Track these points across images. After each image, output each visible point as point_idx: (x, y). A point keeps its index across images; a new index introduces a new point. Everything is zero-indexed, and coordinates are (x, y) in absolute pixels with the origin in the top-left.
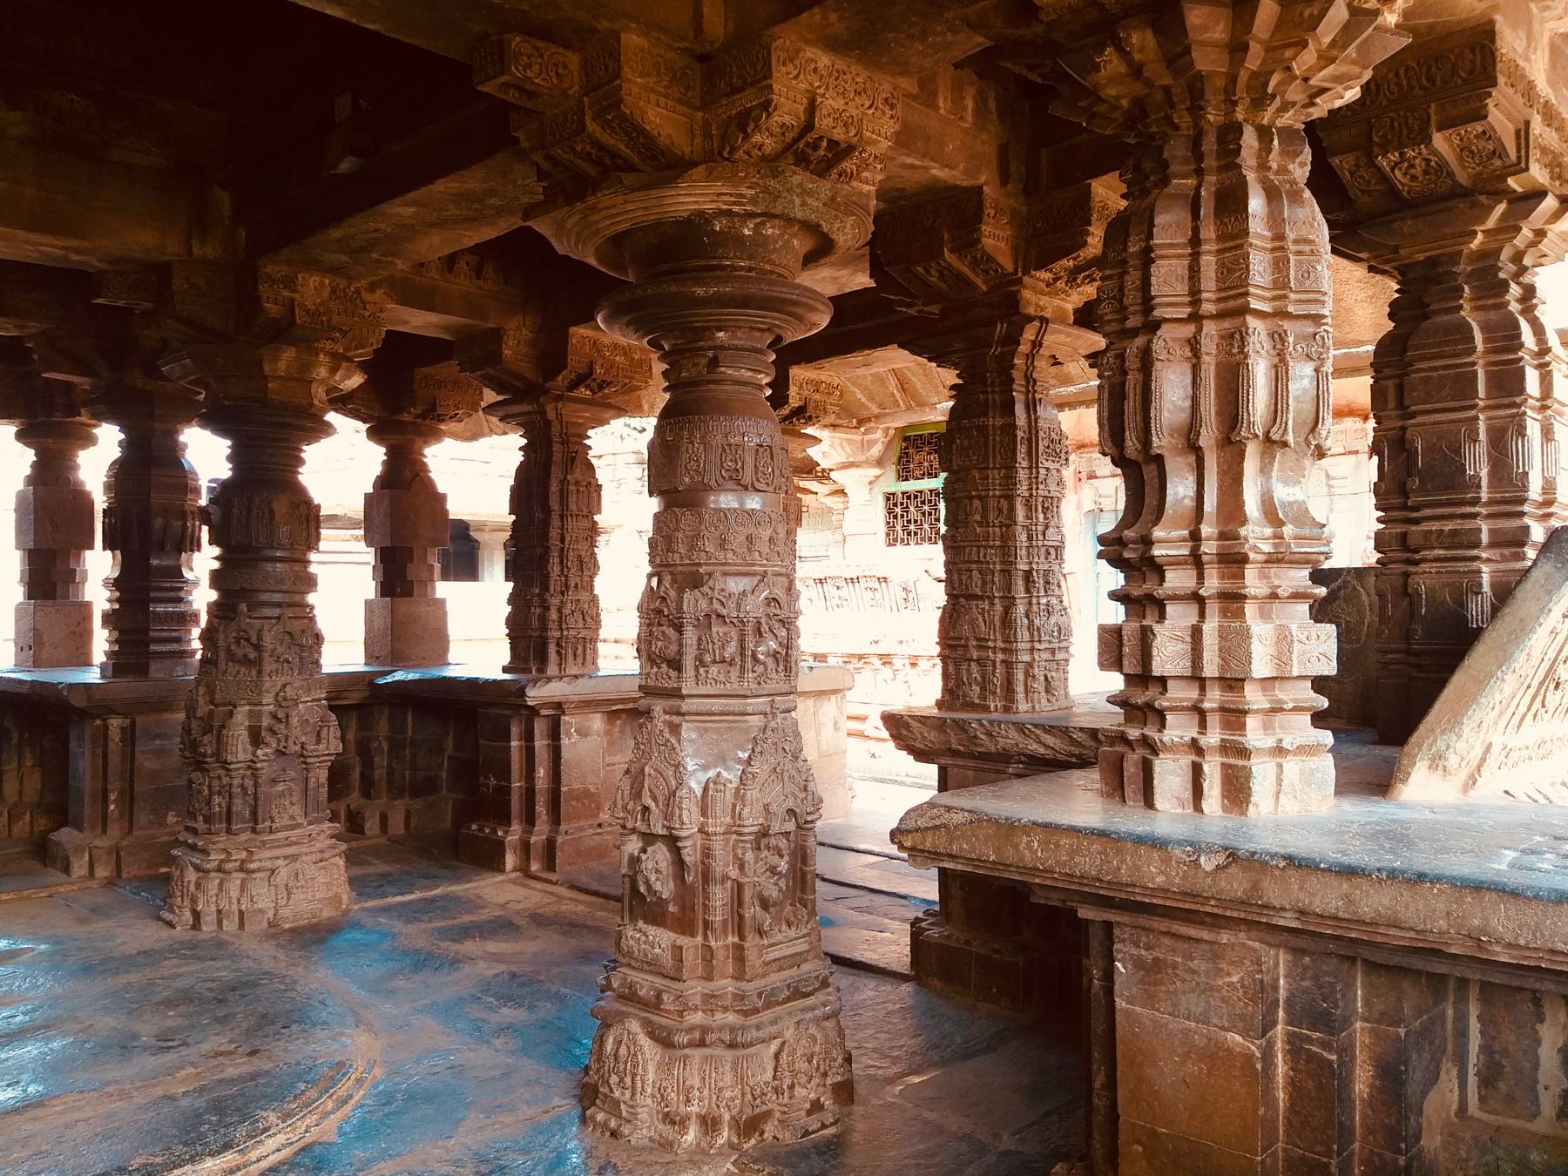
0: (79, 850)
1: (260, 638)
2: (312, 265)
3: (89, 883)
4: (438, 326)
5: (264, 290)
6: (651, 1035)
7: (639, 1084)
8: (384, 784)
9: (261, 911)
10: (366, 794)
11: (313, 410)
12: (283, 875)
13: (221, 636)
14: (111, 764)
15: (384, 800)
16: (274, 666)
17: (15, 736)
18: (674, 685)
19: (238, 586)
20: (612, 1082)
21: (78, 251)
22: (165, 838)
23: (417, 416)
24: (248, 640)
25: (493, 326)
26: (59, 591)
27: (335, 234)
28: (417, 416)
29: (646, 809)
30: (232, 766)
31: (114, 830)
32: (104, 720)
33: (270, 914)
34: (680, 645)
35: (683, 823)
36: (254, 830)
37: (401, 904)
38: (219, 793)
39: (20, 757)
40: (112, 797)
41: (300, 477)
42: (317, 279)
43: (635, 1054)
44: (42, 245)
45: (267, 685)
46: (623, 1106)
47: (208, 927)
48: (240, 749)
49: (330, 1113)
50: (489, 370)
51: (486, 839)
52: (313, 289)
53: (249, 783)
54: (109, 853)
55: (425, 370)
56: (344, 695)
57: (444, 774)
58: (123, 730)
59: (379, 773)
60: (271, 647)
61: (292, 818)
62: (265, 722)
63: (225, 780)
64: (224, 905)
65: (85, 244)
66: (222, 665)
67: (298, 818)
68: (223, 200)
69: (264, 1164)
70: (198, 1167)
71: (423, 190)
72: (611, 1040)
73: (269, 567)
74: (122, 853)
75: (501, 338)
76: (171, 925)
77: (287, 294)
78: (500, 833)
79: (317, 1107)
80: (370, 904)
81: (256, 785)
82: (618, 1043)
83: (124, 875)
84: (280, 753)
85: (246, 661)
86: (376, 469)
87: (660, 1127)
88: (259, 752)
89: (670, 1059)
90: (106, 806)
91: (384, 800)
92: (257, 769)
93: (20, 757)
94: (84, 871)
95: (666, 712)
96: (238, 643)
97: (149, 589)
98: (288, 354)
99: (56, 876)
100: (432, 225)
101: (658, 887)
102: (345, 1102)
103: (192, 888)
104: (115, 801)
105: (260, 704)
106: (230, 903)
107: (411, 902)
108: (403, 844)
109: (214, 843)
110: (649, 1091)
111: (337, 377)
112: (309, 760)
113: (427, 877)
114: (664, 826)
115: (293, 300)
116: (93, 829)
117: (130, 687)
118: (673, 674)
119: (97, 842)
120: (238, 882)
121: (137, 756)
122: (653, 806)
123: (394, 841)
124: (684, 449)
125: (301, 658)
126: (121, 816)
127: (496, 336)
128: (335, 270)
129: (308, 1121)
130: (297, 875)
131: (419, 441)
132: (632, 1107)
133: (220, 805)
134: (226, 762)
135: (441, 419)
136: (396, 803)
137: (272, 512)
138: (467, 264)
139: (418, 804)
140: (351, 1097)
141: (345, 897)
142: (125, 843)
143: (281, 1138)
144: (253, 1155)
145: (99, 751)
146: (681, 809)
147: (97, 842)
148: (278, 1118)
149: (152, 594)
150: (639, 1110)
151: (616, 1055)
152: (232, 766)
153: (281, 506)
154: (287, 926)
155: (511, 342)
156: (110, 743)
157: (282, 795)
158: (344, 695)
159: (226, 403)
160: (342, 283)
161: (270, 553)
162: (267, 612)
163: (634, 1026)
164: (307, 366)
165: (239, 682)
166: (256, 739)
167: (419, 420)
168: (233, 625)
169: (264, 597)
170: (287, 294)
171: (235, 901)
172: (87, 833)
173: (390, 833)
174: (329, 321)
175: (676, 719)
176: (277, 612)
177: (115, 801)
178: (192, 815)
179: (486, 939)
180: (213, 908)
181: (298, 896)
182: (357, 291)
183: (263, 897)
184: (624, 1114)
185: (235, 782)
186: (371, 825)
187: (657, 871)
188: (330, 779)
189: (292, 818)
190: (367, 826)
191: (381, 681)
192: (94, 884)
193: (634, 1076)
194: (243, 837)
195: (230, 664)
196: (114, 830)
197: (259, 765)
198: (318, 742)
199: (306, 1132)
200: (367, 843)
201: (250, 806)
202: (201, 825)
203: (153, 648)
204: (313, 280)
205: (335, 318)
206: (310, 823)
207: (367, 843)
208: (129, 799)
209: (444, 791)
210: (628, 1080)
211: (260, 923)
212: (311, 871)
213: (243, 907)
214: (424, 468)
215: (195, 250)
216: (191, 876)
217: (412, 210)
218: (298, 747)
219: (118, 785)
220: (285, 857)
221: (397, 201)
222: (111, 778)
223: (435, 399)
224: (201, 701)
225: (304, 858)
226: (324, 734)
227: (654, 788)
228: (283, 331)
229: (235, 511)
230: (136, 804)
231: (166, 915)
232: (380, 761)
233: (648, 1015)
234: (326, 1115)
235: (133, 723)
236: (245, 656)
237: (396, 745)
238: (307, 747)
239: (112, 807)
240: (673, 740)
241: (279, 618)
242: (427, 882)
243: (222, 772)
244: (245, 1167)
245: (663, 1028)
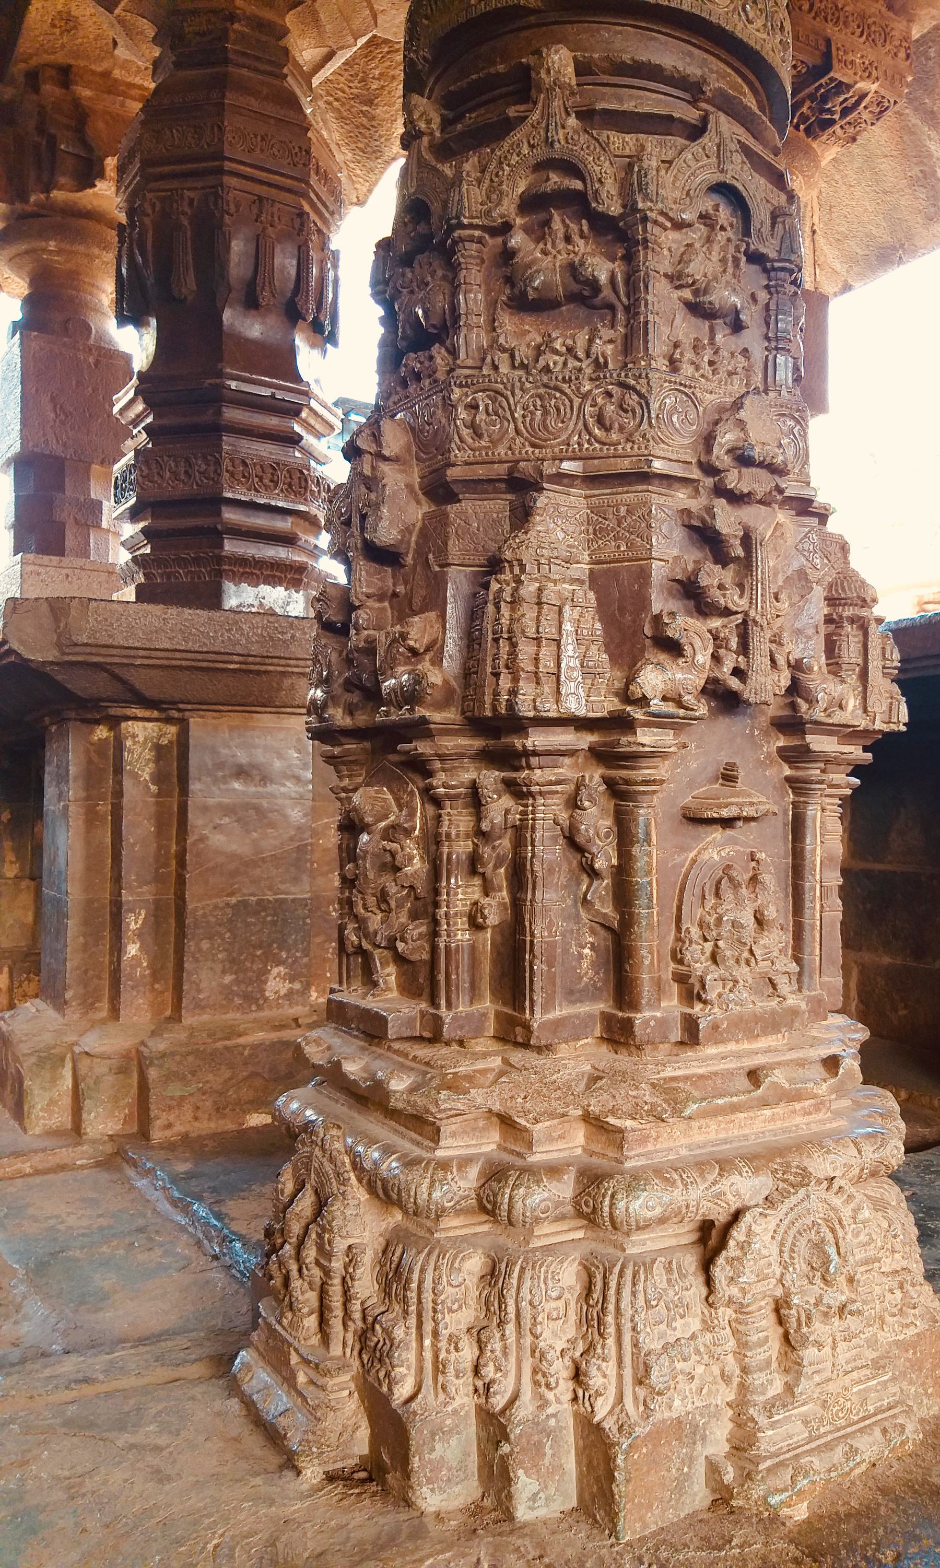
3: (65, 1155)
22: (260, 1036)
26: (70, 542)
40: (134, 922)
58: (160, 751)
74: (153, 1074)
83: (157, 1135)
90: (117, 948)
94: (61, 1118)
104: (140, 934)
116: (88, 1004)
119: (92, 1042)
121: (195, 819)
126: (156, 975)
133: (475, 923)
142: (159, 1045)
145: (104, 807)
147: (92, 1042)
152: (537, 739)
156: (127, 783)
172: (73, 1014)
177: (140, 934)
192: (81, 1155)
195: (508, 322)
203: (230, 546)
219: (147, 892)
222: (130, 875)
223: (828, 42)
230: (191, 946)
235: (184, 735)
239: (132, 950)
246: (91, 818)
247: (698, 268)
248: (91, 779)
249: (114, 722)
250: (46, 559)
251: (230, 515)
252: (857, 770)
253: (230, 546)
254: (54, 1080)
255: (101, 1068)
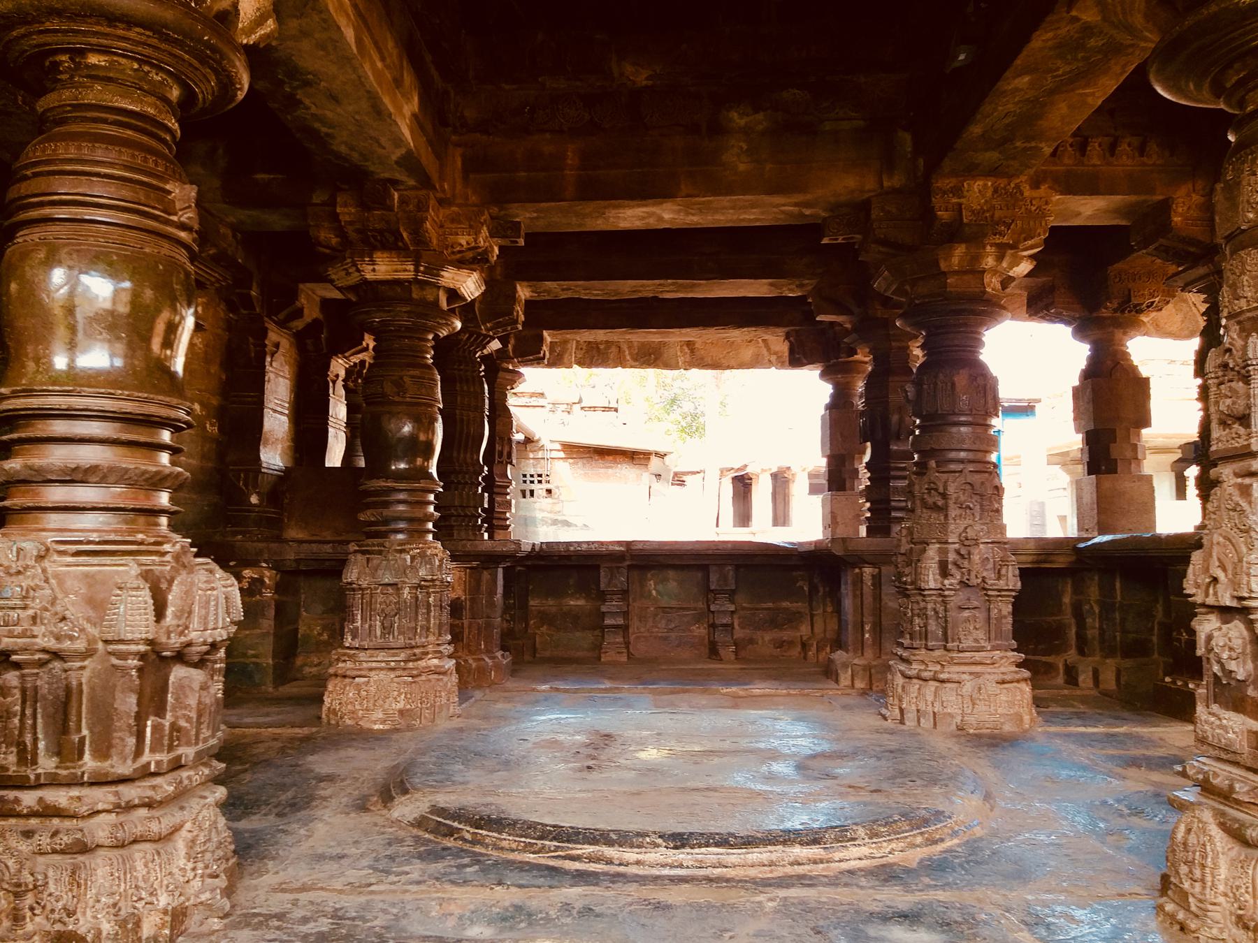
0: (845, 666)
1: (945, 488)
2: (972, 171)
3: (849, 691)
4: (1106, 211)
5: (936, 201)
6: (1223, 826)
7: (1209, 878)
8: (1096, 643)
9: (951, 716)
10: (1081, 652)
11: (986, 297)
12: (968, 687)
13: (917, 487)
14: (865, 602)
15: (1097, 658)
16: (958, 512)
17: (821, 589)
18: (1242, 442)
19: (928, 448)
20: (1181, 872)
21: (807, 205)
23: (1115, 311)
24: (936, 490)
25: (1161, 198)
26: (848, 485)
27: (976, 130)
28: (1115, 311)
29: (1215, 580)
30: (926, 593)
31: (869, 653)
32: (860, 568)
33: (958, 719)
34: (1248, 397)
35: (1251, 591)
36: (945, 648)
37: (1083, 735)
38: (919, 616)
39: (825, 605)
40: (867, 628)
41: (982, 357)
42: (981, 183)
43: (1204, 845)
44: (784, 205)
45: (952, 527)
46: (1191, 899)
47: (910, 722)
48: (931, 580)
49: (918, 846)
50: (1162, 241)
51: (1178, 690)
52: (977, 192)
53: (941, 609)
54: (864, 670)
55: (1119, 266)
56: (1052, 558)
57: (1155, 639)
58: (873, 576)
59: (1092, 633)
60: (955, 495)
61: (976, 640)
62: (952, 557)
63: (922, 604)
64: (922, 706)
65: (809, 197)
66: (918, 511)
67: (982, 641)
68: (906, 140)
69: (844, 866)
70: (787, 849)
71: (1024, 53)
72: (1182, 828)
73: (954, 429)
74: (873, 671)
75: (1170, 207)
76: (885, 718)
77: (955, 200)
78: (1191, 686)
79: (906, 837)
80: (1053, 729)
81: (946, 611)
82: (1189, 831)
83: (874, 688)
84: (964, 584)
85: (935, 508)
86: (1082, 363)
87: (1234, 930)
88: (946, 582)
89: (1246, 857)
90: (863, 635)
91: (1097, 658)
92: (945, 596)
93: (825, 605)
94: (848, 683)
95: (1237, 475)
96: (929, 493)
97: (889, 469)
98: (960, 251)
99: (832, 685)
100: (1052, 92)
101: (1232, 666)
102: (935, 842)
103: (900, 690)
104: (869, 631)
105: (947, 543)
106: (927, 705)
107: (1094, 734)
108: (1111, 697)
109: (914, 655)
110: (1221, 888)
111: (1005, 264)
112: (990, 593)
113: (1117, 718)
114: (1234, 597)
115: (960, 205)
116: (855, 651)
117: (879, 542)
118: (1242, 431)
119: (856, 661)
120: (933, 689)
122: (1220, 575)
123: (1105, 694)
124: (1244, 183)
125: (982, 505)
127: (1165, 207)
128: (994, 172)
129: (893, 845)
130: (980, 689)
131: (1118, 334)
132: (1200, 901)
134: (920, 589)
135: (1140, 311)
136: (1107, 661)
137: (953, 384)
138: (1129, 145)
139: (1128, 663)
140: (942, 840)
141: (1027, 718)
142: (875, 663)
143: (865, 851)
144: (837, 856)
146: (1248, 575)
147: (856, 661)
148: (866, 834)
149: (892, 473)
150: (1210, 907)
151: (1185, 844)
152: (926, 593)
153: (961, 379)
154: (971, 731)
155: (1180, 210)
156: (864, 587)
157: (967, 620)
158: (1052, 558)
159: (917, 302)
160: (1002, 182)
161: (956, 419)
162: (953, 467)
163: (1207, 816)
164: (976, 258)
165: (930, 525)
166: (944, 572)
167: (1118, 314)
168: (926, 478)
169: (953, 455)
170: (955, 200)
171: (929, 703)
172: (851, 654)
173: (1101, 686)
174: (992, 216)
175: (1247, 481)
176: (961, 466)
177: (869, 631)
178: (902, 634)
179: (1151, 769)
180: (914, 708)
181: (981, 707)
182: (1017, 186)
183: (951, 703)
184: (1193, 908)
185: (930, 606)
186: (1085, 679)
187: (1231, 649)
188: (1015, 612)
189: (976, 640)
190: (1081, 678)
191: (1082, 545)
193: (1203, 866)
194: (937, 653)
195: (924, 510)
196: (869, 653)
197: (946, 593)
198: (999, 578)
199: (890, 853)
200: (1078, 692)
201: (942, 627)
202: (906, 642)
203: (894, 514)
204: (978, 185)
205: (998, 214)
206: (994, 648)
207: (1078, 692)
208: (878, 629)
209: (1156, 656)
210: (1198, 873)
211: (950, 724)
212: (992, 688)
213: (936, 710)
214: (1126, 356)
215: (886, 184)
216: (899, 680)
217: (1026, 79)
218: (979, 580)
220: (971, 674)
221: (1008, 74)
222: (866, 613)
223: (1129, 290)
224: (904, 540)
225: (987, 676)
226: (1003, 571)
227: (1222, 557)
228: (954, 233)
229: (925, 387)
230: (883, 635)
231: (884, 711)
232: (1093, 624)
233: (1222, 807)
234: (914, 846)
236: (934, 503)
237: (1107, 608)
238: (987, 581)
239: (867, 636)
240: (1244, 505)
241: (961, 472)
242: (1111, 721)
243: (920, 598)
244: (828, 862)
245: (1236, 820)
246: (855, 596)
247: (962, 498)
248: (854, 584)
249: (860, 568)
250: (839, 493)
251: (893, 504)
252: (1014, 597)
253: (894, 514)
254: (846, 672)
255: (859, 668)
